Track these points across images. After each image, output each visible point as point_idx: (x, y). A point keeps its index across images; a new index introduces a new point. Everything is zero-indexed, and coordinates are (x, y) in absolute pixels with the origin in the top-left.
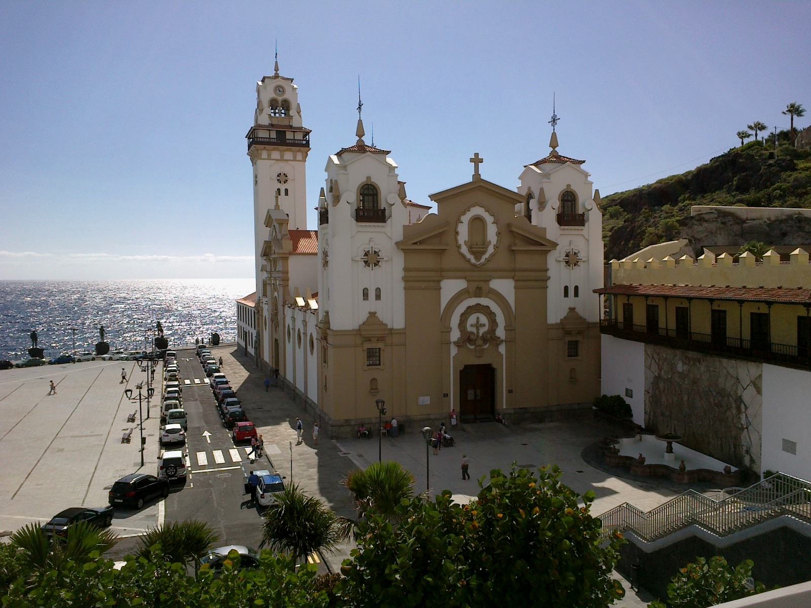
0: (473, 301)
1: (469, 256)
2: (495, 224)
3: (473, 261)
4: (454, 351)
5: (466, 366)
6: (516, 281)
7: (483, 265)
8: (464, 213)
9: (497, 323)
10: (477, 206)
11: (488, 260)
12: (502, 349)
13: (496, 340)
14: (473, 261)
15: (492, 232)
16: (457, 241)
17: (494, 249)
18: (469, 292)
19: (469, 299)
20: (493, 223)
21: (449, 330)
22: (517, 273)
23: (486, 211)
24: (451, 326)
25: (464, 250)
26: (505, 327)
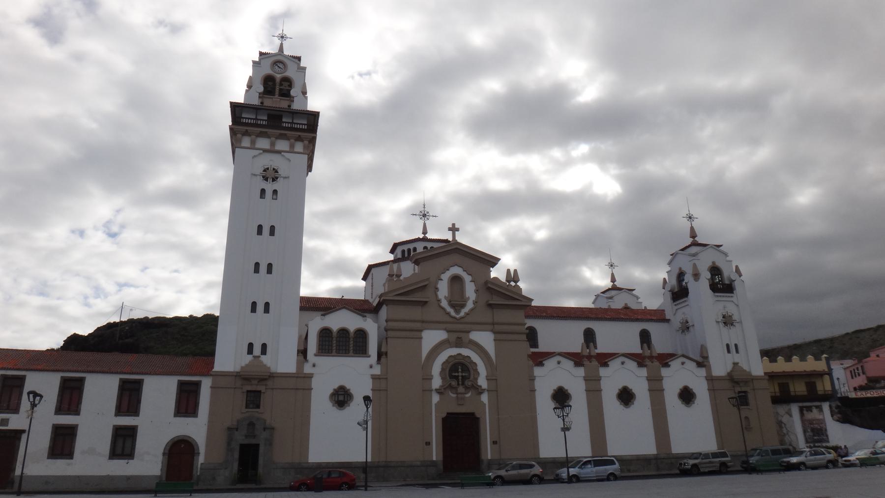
0: (453, 351)
2: (473, 283)
3: (453, 313)
4: (436, 398)
5: (448, 413)
6: (495, 333)
7: (462, 318)
9: (478, 372)
10: (456, 267)
11: (467, 314)
12: (485, 398)
13: (478, 388)
14: (453, 313)
15: (470, 290)
16: (436, 295)
17: (474, 304)
18: (449, 342)
20: (471, 281)
24: (433, 373)
25: (444, 304)
26: (486, 376)
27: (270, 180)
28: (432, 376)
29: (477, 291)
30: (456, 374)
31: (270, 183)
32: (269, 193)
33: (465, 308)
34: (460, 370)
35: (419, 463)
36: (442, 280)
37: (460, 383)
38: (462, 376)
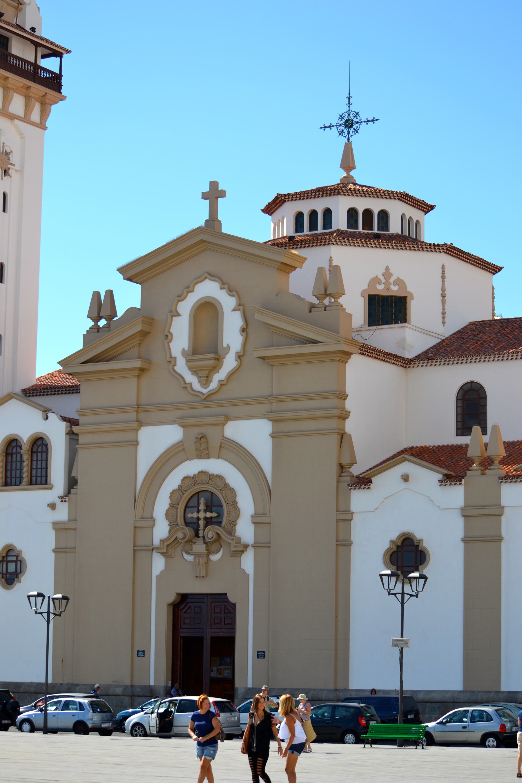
1: (190, 378)
3: (197, 386)
8: (181, 297)
11: (222, 384)
14: (197, 386)
20: (234, 310)
21: (150, 523)
22: (275, 406)
23: (221, 288)
25: (182, 367)
28: (154, 520)
29: (243, 330)
30: (195, 515)
33: (220, 371)
34: (202, 507)
35: (119, 691)
36: (179, 315)
37: (201, 533)
38: (198, 519)
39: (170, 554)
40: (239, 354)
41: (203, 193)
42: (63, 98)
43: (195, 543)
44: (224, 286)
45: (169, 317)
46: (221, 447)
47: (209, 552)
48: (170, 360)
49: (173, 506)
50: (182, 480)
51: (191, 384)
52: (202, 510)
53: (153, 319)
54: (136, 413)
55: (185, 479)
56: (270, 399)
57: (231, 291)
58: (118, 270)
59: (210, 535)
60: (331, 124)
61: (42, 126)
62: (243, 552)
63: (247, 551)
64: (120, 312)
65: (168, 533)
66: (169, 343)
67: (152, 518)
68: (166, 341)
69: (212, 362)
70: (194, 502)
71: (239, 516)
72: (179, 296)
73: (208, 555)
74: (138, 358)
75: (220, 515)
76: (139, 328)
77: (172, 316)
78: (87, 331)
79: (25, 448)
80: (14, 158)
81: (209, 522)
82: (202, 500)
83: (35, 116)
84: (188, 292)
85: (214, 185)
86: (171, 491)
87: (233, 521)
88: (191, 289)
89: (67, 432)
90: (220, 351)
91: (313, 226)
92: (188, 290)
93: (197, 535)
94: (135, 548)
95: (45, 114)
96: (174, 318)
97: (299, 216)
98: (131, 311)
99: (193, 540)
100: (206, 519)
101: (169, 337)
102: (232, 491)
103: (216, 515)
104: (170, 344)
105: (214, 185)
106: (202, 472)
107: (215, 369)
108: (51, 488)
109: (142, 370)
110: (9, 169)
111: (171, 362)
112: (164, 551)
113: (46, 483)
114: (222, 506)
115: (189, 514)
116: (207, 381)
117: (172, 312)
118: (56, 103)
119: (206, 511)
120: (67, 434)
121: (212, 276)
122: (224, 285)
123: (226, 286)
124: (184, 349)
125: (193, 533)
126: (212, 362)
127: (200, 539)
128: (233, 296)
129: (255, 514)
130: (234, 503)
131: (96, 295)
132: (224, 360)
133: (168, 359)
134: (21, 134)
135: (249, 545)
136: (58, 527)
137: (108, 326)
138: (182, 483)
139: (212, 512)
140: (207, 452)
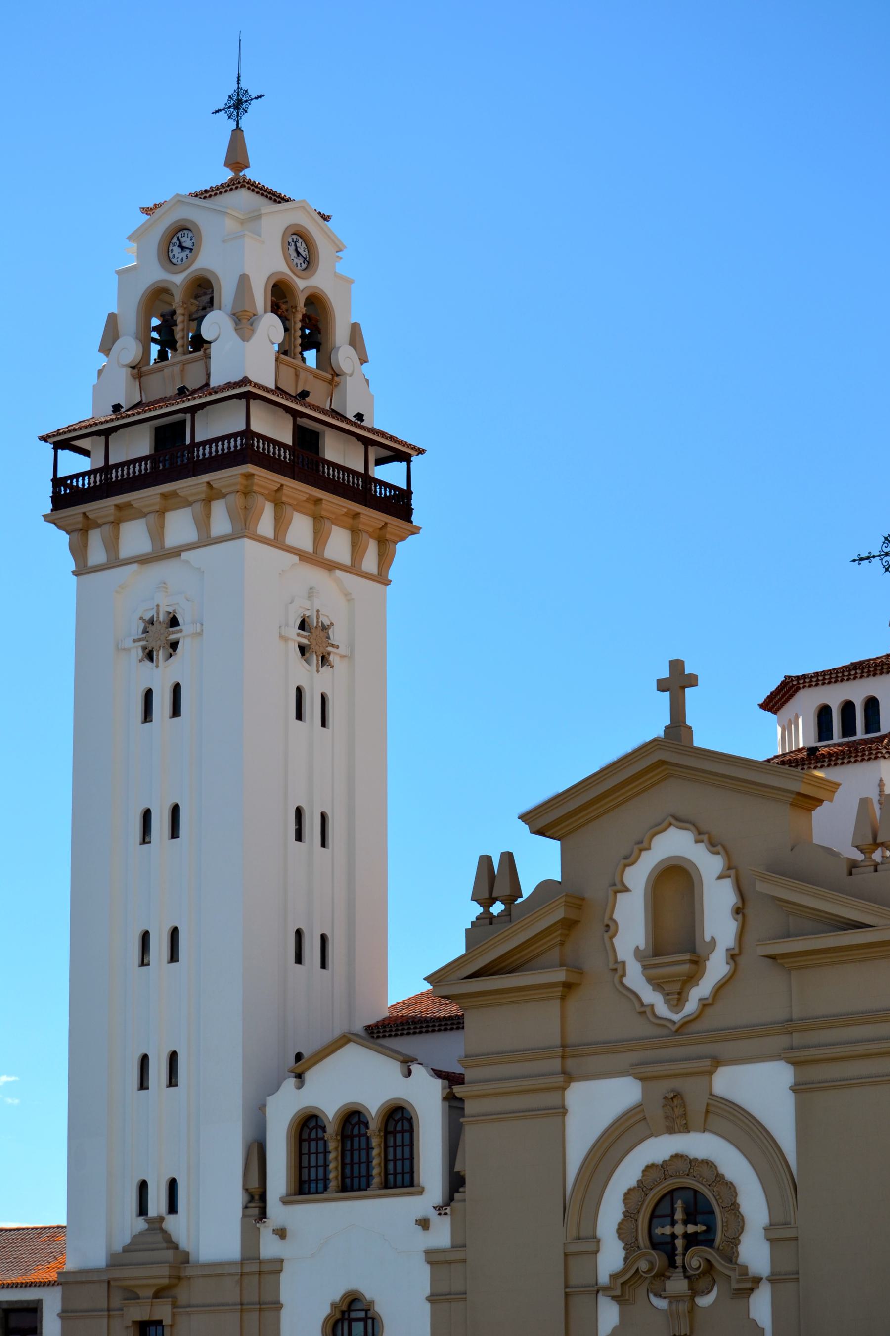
1: (651, 996)
3: (662, 1010)
8: (630, 860)
11: (705, 1005)
14: (662, 1010)
19: (653, 1138)
20: (720, 877)
21: (592, 1247)
22: (797, 1039)
23: (697, 842)
27: (160, 655)
28: (599, 1241)
29: (738, 911)
30: (668, 1230)
31: (157, 666)
32: (162, 703)
34: (679, 1215)
36: (627, 890)
37: (679, 1259)
39: (627, 1298)
40: (733, 952)
41: (659, 681)
42: (416, 531)
43: (669, 1278)
44: (701, 837)
45: (611, 893)
46: (707, 1112)
47: (695, 1292)
48: (614, 967)
49: (630, 1215)
50: (643, 1171)
51: (652, 1007)
52: (680, 1222)
53: (583, 899)
54: (560, 1059)
55: (649, 1168)
56: (789, 1026)
57: (714, 845)
58: (519, 818)
59: (695, 1263)
60: (870, 553)
61: (382, 578)
62: (752, 1290)
63: (758, 1288)
64: (527, 889)
65: (623, 1263)
66: (611, 938)
67: (595, 1237)
68: (606, 936)
69: (686, 968)
70: (665, 1208)
71: (743, 1228)
72: (626, 858)
73: (692, 1298)
74: (561, 966)
75: (710, 1229)
76: (559, 914)
77: (616, 892)
78: (472, 923)
79: (374, 1125)
80: (338, 635)
81: (691, 1240)
82: (679, 1204)
83: (370, 563)
84: (641, 850)
85: (676, 666)
86: (625, 1190)
87: (734, 1238)
88: (645, 845)
89: (445, 1095)
90: (699, 948)
91: (848, 728)
92: (641, 846)
93: (672, 1264)
94: (567, 1290)
95: (385, 558)
96: (619, 895)
97: (824, 713)
98: (545, 887)
99: (667, 1274)
100: (686, 1235)
101: (612, 928)
102: (730, 1187)
103: (704, 1228)
104: (614, 940)
105: (676, 666)
106: (677, 1157)
107: (693, 978)
108: (421, 1193)
109: (568, 986)
110: (329, 654)
111: (615, 970)
112: (618, 1292)
113: (412, 1184)
114: (712, 1212)
115: (657, 1228)
116: (679, 999)
117: (614, 885)
118: (403, 539)
119: (686, 1222)
120: (445, 1099)
121: (681, 821)
122: (702, 835)
123: (705, 837)
124: (638, 947)
125: (665, 1260)
126: (686, 968)
127: (677, 1270)
128: (718, 853)
129: (771, 1225)
130: (734, 1208)
131: (485, 861)
132: (707, 963)
133: (612, 966)
134: (347, 595)
135: (761, 1279)
136: (434, 1258)
137: (507, 914)
138: (643, 1176)
139: (696, 1224)
140: (685, 1122)
